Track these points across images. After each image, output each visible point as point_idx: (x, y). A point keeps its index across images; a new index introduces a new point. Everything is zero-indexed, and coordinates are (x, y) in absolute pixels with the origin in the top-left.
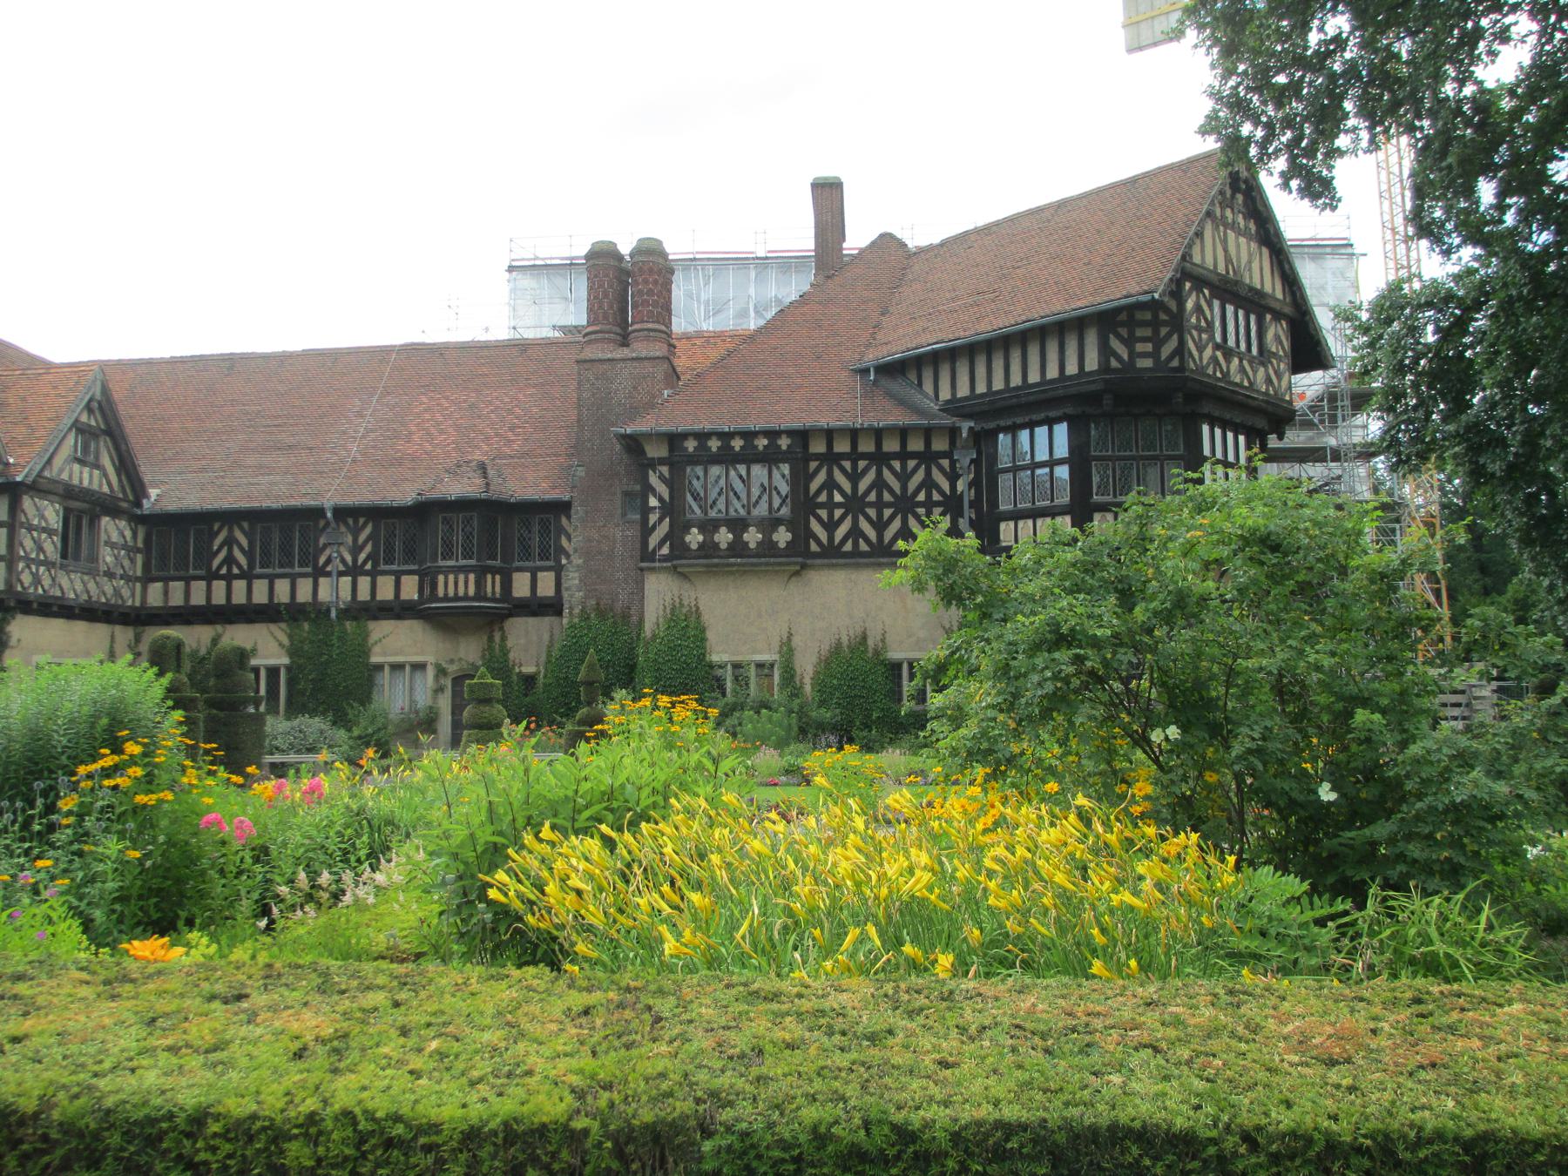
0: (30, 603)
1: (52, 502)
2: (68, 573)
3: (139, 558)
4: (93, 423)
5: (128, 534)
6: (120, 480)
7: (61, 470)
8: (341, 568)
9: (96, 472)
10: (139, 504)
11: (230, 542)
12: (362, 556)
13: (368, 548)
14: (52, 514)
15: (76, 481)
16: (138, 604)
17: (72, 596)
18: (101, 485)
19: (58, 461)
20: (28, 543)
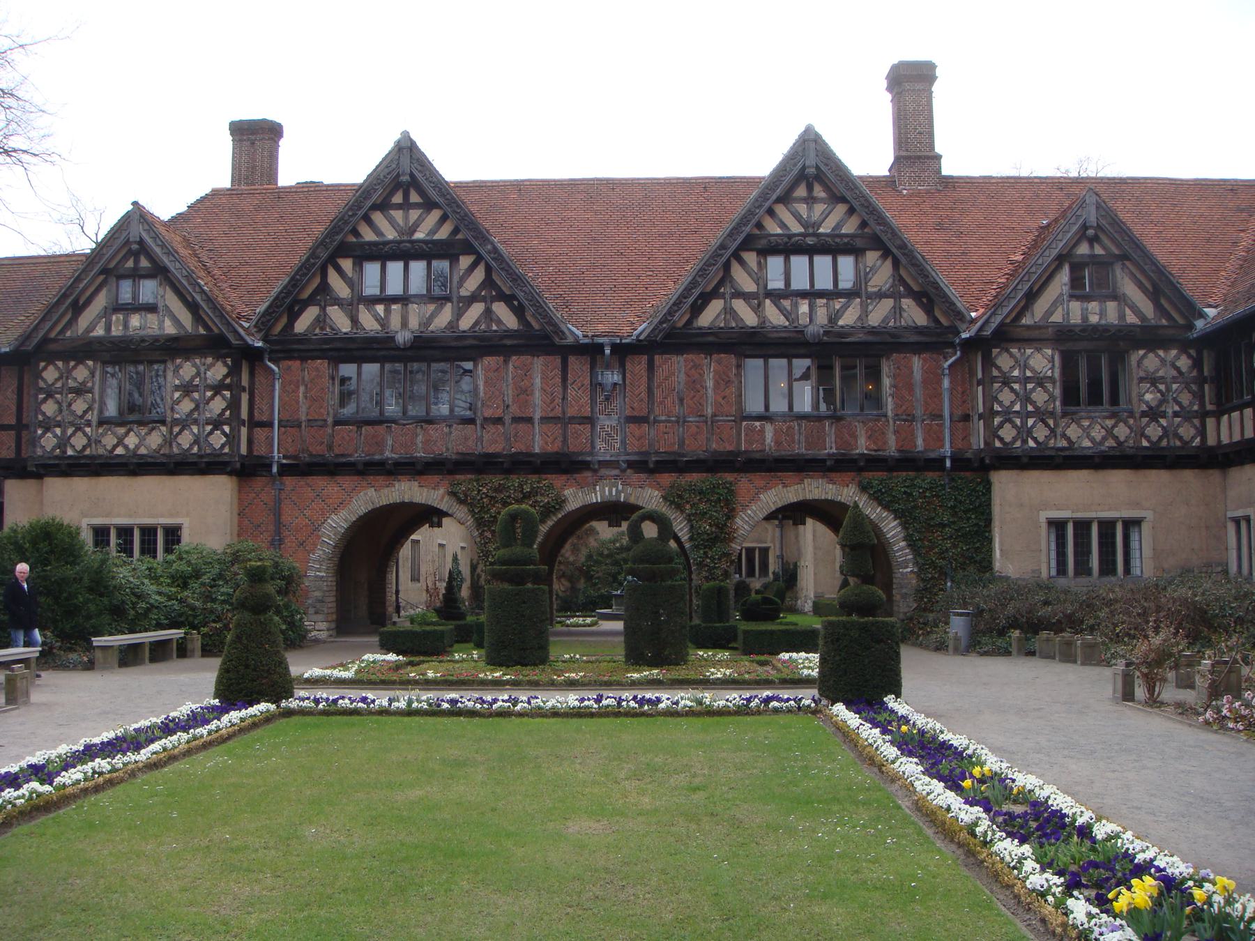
1: (1038, 350)
4: (1098, 250)
5: (1184, 363)
7: (1049, 313)
9: (1111, 306)
10: (1191, 327)
14: (1043, 361)
15: (1076, 319)
16: (1211, 441)
17: (1087, 443)
18: (1122, 316)
19: (1041, 306)
20: (1006, 397)
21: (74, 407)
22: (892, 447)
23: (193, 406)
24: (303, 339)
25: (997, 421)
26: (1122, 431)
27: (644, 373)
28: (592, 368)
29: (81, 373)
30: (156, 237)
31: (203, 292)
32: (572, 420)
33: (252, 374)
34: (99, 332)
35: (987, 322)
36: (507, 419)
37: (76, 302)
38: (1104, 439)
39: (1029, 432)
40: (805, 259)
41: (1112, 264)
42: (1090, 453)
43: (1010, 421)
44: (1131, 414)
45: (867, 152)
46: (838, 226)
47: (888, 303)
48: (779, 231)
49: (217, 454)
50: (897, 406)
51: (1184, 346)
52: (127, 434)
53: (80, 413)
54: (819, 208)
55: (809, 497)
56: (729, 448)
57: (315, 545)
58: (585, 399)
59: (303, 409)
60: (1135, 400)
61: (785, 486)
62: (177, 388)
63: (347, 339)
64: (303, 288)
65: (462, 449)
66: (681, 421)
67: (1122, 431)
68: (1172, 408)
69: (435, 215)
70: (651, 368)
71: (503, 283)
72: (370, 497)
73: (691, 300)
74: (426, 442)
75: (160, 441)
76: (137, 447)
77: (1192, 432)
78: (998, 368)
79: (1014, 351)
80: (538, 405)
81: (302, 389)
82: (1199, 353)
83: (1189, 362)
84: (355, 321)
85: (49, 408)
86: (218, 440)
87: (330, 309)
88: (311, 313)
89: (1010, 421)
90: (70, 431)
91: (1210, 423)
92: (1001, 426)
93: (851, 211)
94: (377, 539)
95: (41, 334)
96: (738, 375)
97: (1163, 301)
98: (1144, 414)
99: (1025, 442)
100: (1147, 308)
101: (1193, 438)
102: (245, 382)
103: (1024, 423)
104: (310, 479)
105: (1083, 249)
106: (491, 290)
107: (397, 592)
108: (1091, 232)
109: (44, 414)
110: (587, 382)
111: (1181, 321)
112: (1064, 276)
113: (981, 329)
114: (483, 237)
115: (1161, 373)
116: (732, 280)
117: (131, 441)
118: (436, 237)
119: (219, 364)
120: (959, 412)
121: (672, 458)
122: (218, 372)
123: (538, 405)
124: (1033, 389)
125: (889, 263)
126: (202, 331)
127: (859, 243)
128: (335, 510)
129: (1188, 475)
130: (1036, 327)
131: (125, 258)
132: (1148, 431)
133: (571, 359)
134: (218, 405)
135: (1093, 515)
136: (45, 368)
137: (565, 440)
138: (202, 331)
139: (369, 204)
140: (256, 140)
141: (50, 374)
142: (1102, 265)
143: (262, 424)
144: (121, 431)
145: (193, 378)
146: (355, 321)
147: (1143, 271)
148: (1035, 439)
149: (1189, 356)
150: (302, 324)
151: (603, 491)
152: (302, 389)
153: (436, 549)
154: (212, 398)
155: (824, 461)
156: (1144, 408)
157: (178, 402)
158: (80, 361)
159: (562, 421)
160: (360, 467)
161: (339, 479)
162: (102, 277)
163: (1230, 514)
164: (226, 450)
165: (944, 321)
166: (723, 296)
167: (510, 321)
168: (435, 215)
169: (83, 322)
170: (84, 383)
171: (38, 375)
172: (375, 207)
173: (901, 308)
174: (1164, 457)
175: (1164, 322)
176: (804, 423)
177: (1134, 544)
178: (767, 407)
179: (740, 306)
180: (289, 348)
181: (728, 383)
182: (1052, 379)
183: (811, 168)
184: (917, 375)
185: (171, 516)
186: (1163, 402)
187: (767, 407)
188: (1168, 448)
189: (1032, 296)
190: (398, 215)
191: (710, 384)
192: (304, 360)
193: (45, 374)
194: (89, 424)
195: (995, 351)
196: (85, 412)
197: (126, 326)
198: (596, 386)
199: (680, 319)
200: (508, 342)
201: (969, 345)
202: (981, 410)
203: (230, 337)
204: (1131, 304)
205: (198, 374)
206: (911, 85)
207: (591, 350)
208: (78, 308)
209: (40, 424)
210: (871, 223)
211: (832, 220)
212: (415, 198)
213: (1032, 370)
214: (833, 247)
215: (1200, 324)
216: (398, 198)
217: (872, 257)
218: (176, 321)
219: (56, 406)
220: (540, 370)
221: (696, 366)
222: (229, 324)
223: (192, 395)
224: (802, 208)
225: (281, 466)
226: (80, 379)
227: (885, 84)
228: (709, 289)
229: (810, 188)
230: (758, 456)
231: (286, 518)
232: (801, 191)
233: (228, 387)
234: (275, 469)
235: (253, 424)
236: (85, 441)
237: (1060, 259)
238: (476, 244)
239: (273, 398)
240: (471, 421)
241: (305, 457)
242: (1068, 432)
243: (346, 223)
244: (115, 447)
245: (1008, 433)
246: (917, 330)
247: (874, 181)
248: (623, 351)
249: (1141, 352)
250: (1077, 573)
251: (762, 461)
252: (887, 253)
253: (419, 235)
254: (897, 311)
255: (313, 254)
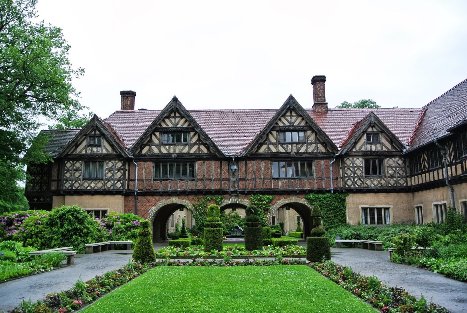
0: (353, 190)
1: (358, 159)
2: (370, 179)
3: (408, 170)
4: (375, 130)
5: (400, 162)
6: (392, 145)
7: (361, 148)
8: (448, 164)
9: (379, 146)
10: (402, 151)
11: (424, 159)
12: (452, 157)
13: (453, 154)
14: (359, 162)
15: (368, 149)
16: (409, 184)
17: (372, 186)
19: (358, 146)
20: (349, 172)
21: (75, 175)
22: (316, 187)
23: (111, 175)
24: (144, 156)
25: (346, 179)
26: (383, 182)
27: (244, 166)
28: (229, 165)
29: (78, 165)
30: (102, 124)
31: (115, 141)
32: (223, 180)
33: (129, 166)
34: (84, 152)
35: (343, 151)
36: (204, 180)
37: (77, 143)
38: (378, 184)
39: (356, 183)
40: (290, 133)
41: (378, 134)
42: (373, 188)
43: (350, 179)
44: (385, 176)
45: (306, 101)
46: (299, 123)
47: (314, 146)
48: (282, 125)
49: (119, 189)
50: (317, 175)
51: (400, 157)
52: (91, 183)
53: (77, 176)
54: (294, 118)
55: (292, 201)
56: (269, 188)
57: (147, 216)
58: (227, 174)
59: (144, 176)
60: (386, 173)
61: (285, 199)
62: (107, 169)
63: (157, 155)
64: (145, 140)
65: (191, 188)
66: (255, 180)
67: (383, 182)
68: (397, 175)
69: (183, 120)
70: (246, 164)
71: (204, 139)
72: (164, 202)
73: (257, 145)
74: (181, 186)
75: (101, 185)
76: (94, 187)
77: (403, 182)
78: (346, 164)
79: (351, 159)
80: (214, 175)
81: (144, 170)
82: (405, 159)
83: (402, 162)
84: (160, 150)
85: (68, 175)
86: (119, 185)
87: (152, 147)
88: (147, 148)
89: (350, 179)
90: (74, 182)
91: (409, 179)
92: (347, 181)
93: (303, 119)
94: (164, 214)
95: (66, 152)
96: (271, 167)
97: (394, 144)
98: (389, 177)
99: (354, 185)
100: (389, 146)
101: (404, 183)
102: (127, 168)
103: (354, 180)
104: (146, 197)
105: (370, 129)
106: (200, 142)
107: (168, 230)
108: (372, 125)
109: (66, 177)
110: (227, 168)
111: (399, 150)
112: (365, 137)
113: (341, 153)
114: (198, 126)
115: (394, 165)
116: (269, 139)
117: (93, 185)
118: (184, 126)
119: (120, 163)
120: (335, 177)
121: (252, 190)
122: (119, 165)
123: (214, 175)
124: (356, 170)
125: (314, 134)
126: (114, 153)
127: (305, 128)
128: (153, 206)
129: (403, 195)
130: (357, 152)
131: (92, 131)
132: (390, 182)
133: (223, 162)
134: (119, 175)
135: (375, 206)
136: (67, 163)
137: (221, 186)
138: (114, 153)
139: (164, 116)
140: (128, 97)
141: (68, 165)
142: (377, 134)
143: (132, 180)
144: (90, 182)
145: (112, 167)
146: (160, 150)
147: (388, 136)
148: (357, 185)
149: (402, 160)
150: (145, 151)
151: (232, 200)
152: (144, 170)
153: (178, 217)
154: (117, 172)
155: (296, 191)
156: (389, 175)
157: (107, 173)
158: (78, 161)
159: (221, 180)
160: (161, 193)
161: (155, 197)
162: (85, 137)
163: (415, 206)
164: (121, 188)
165: (330, 151)
166: (266, 144)
167: (205, 151)
168: (183, 120)
169: (79, 150)
170: (79, 168)
171: (65, 165)
172: (166, 117)
173: (318, 147)
174: (395, 189)
175: (394, 150)
176: (290, 180)
177: (387, 215)
178: (279, 176)
179: (271, 146)
180: (141, 158)
181: (268, 168)
182: (362, 167)
183: (291, 106)
184: (323, 167)
185: (104, 207)
186: (395, 173)
187: (279, 176)
188: (397, 187)
189: (355, 143)
190: (173, 120)
191: (263, 169)
192: (144, 161)
193: (67, 165)
194: (80, 180)
195: (345, 159)
196: (79, 176)
197: (92, 150)
198: (230, 170)
199: (254, 150)
200: (205, 157)
201: (337, 158)
202: (341, 176)
203: (123, 154)
204: (384, 145)
205: (113, 165)
206: (319, 81)
207: (229, 160)
208: (77, 146)
209: (65, 180)
210: (309, 122)
211: (298, 122)
212: (177, 115)
213: (356, 164)
214: (298, 130)
215: (404, 150)
216: (172, 115)
217: (309, 132)
218: (107, 150)
219: (70, 174)
220: (214, 165)
221: (259, 164)
222: (123, 151)
223: (112, 172)
224: (289, 119)
225: (138, 193)
226: (77, 166)
227: (311, 82)
228: (262, 142)
229: (291, 113)
230: (277, 190)
231: (139, 208)
232: (288, 114)
233: (122, 169)
234: (136, 194)
235: (129, 180)
236: (78, 185)
237: (364, 132)
238: (195, 129)
239: (135, 173)
240: (194, 180)
241: (145, 190)
242: (367, 182)
243: (157, 122)
244: (88, 187)
245: (349, 183)
246: (323, 153)
247: (309, 110)
248: (238, 160)
249: (388, 159)
250: (371, 223)
251: (278, 191)
252: (313, 131)
253: (178, 126)
254: (317, 148)
255: (148, 130)
